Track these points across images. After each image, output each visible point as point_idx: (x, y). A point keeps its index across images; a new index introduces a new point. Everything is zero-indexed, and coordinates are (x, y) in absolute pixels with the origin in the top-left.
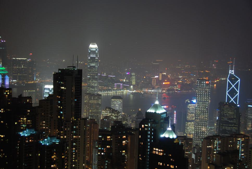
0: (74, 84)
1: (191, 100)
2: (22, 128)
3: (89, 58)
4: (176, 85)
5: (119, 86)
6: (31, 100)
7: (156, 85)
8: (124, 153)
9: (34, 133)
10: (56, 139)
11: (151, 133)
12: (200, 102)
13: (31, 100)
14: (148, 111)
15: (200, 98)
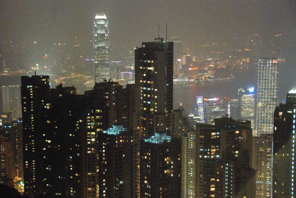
0: (166, 62)
1: (245, 89)
2: (89, 127)
3: (96, 35)
4: (206, 71)
5: (128, 75)
6: (75, 91)
8: (237, 154)
9: (123, 130)
10: (166, 136)
12: (265, 91)
13: (75, 91)
14: (290, 92)
15: (265, 84)
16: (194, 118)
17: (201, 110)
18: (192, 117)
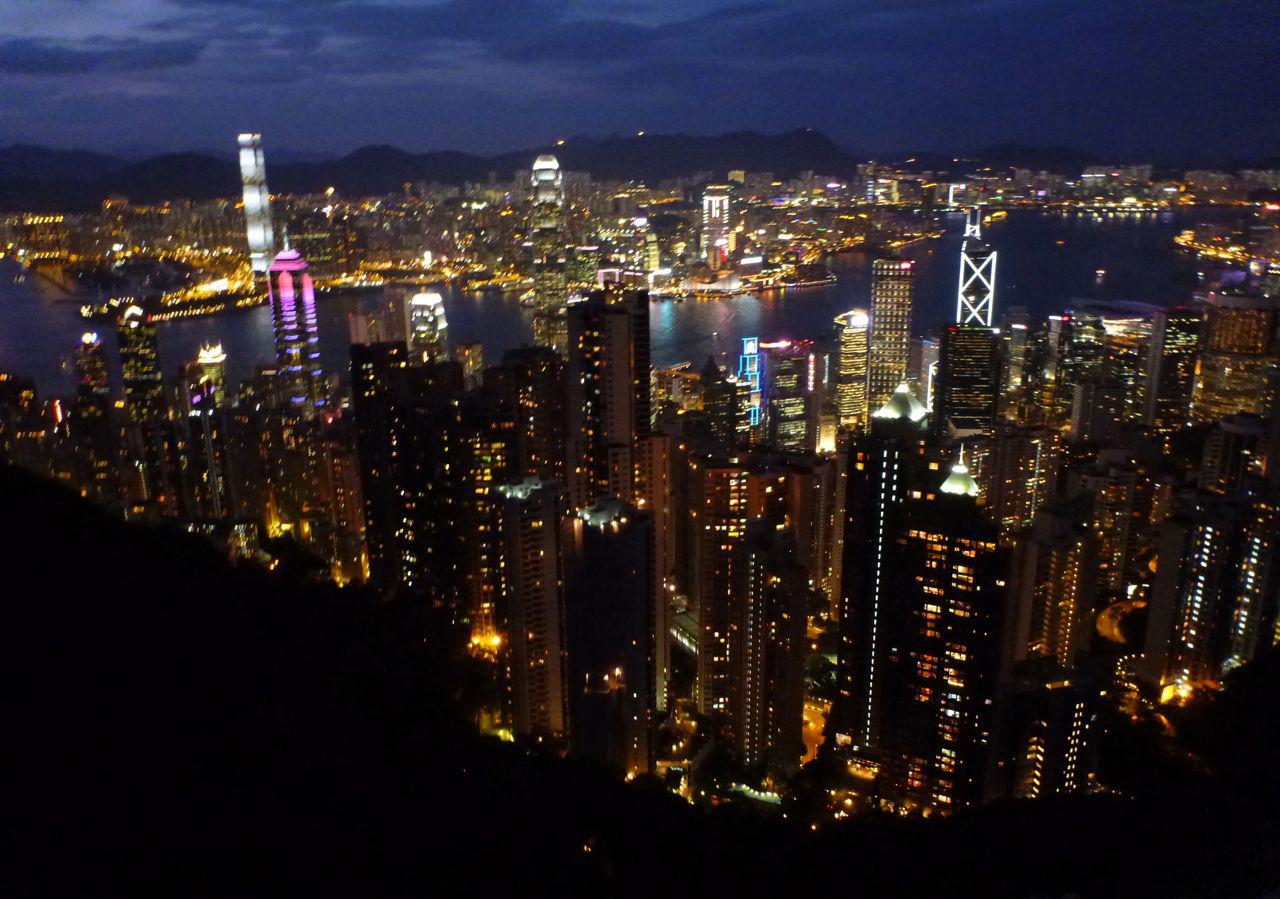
4: (777, 266)
7: (722, 268)
11: (889, 476)
16: (738, 385)
17: (753, 369)
18: (734, 384)
